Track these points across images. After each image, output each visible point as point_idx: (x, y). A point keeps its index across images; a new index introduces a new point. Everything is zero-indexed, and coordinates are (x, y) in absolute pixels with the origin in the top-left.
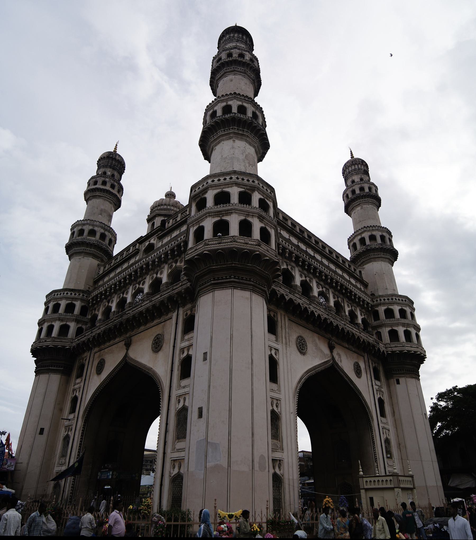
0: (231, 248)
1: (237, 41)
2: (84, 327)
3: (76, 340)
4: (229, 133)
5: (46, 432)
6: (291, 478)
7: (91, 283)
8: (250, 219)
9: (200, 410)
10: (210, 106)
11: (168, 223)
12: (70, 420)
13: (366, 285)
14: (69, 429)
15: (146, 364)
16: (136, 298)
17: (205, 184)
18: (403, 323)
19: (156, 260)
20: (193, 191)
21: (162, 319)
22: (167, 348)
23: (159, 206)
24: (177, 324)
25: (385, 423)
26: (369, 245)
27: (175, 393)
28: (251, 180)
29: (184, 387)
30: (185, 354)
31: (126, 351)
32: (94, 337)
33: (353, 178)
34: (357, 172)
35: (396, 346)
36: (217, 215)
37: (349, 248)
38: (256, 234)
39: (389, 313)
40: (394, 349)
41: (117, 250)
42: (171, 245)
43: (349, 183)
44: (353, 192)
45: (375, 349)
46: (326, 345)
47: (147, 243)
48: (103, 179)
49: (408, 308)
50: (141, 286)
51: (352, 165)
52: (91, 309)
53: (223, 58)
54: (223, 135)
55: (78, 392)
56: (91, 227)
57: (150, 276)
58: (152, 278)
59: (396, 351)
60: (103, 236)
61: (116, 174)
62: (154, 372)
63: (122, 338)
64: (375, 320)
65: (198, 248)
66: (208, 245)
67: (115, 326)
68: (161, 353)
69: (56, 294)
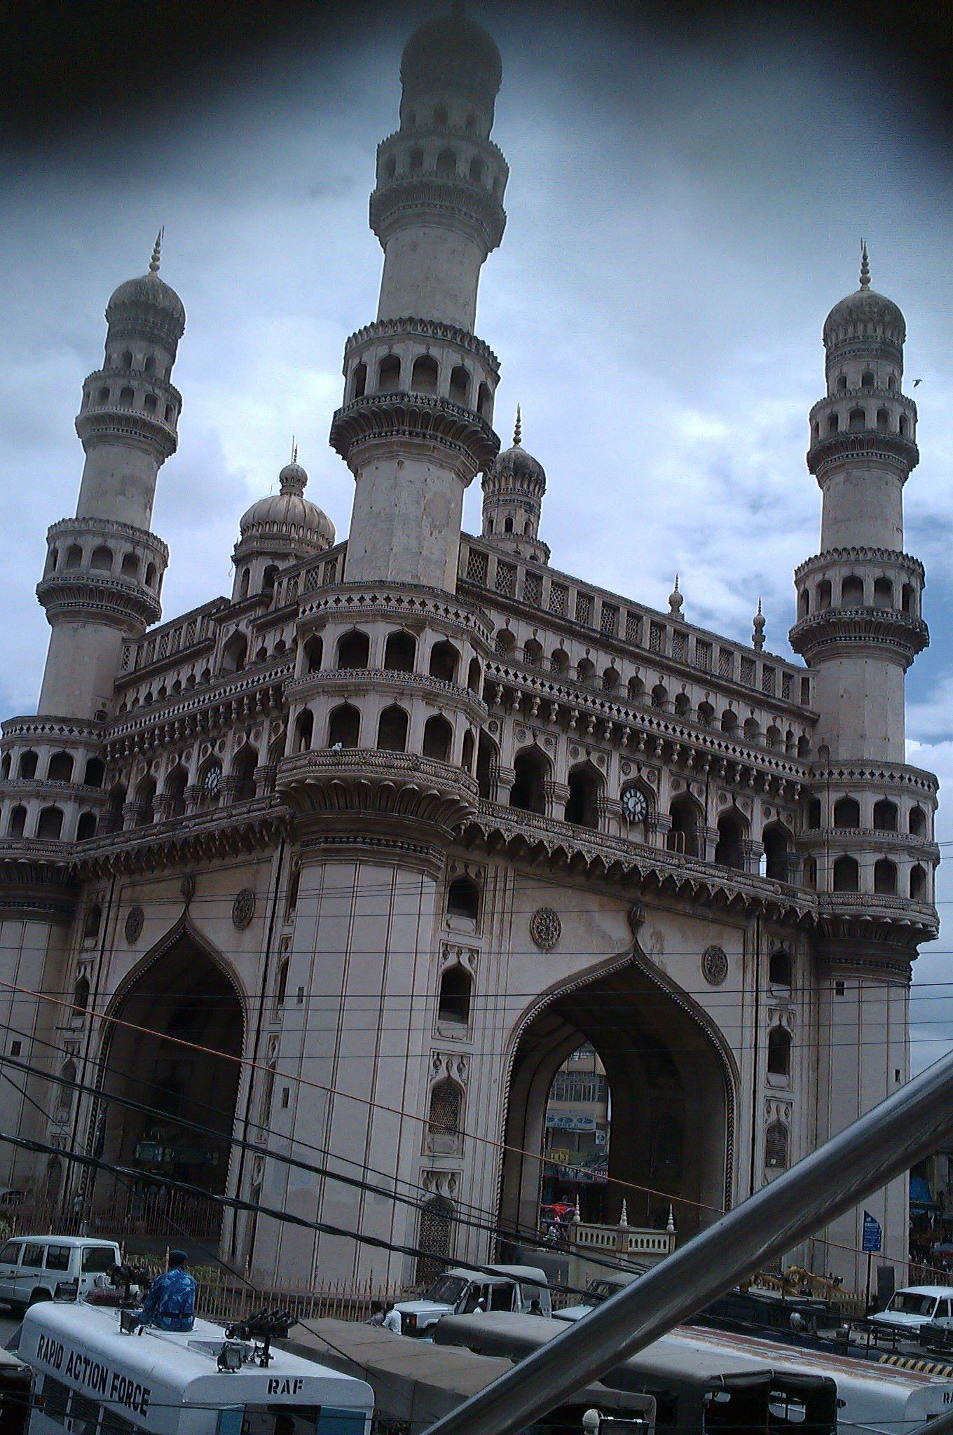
0: (355, 778)
2: (96, 812)
7: (109, 690)
8: (404, 704)
11: (280, 584)
13: (812, 722)
18: (876, 843)
19: (246, 701)
22: (259, 928)
24: (278, 879)
39: (847, 812)
40: (839, 910)
46: (622, 917)
48: (123, 382)
51: (847, 322)
55: (89, 970)
56: (97, 542)
58: (240, 739)
60: (131, 561)
61: (159, 354)
65: (298, 764)
66: (315, 765)
67: (161, 847)
68: (248, 933)
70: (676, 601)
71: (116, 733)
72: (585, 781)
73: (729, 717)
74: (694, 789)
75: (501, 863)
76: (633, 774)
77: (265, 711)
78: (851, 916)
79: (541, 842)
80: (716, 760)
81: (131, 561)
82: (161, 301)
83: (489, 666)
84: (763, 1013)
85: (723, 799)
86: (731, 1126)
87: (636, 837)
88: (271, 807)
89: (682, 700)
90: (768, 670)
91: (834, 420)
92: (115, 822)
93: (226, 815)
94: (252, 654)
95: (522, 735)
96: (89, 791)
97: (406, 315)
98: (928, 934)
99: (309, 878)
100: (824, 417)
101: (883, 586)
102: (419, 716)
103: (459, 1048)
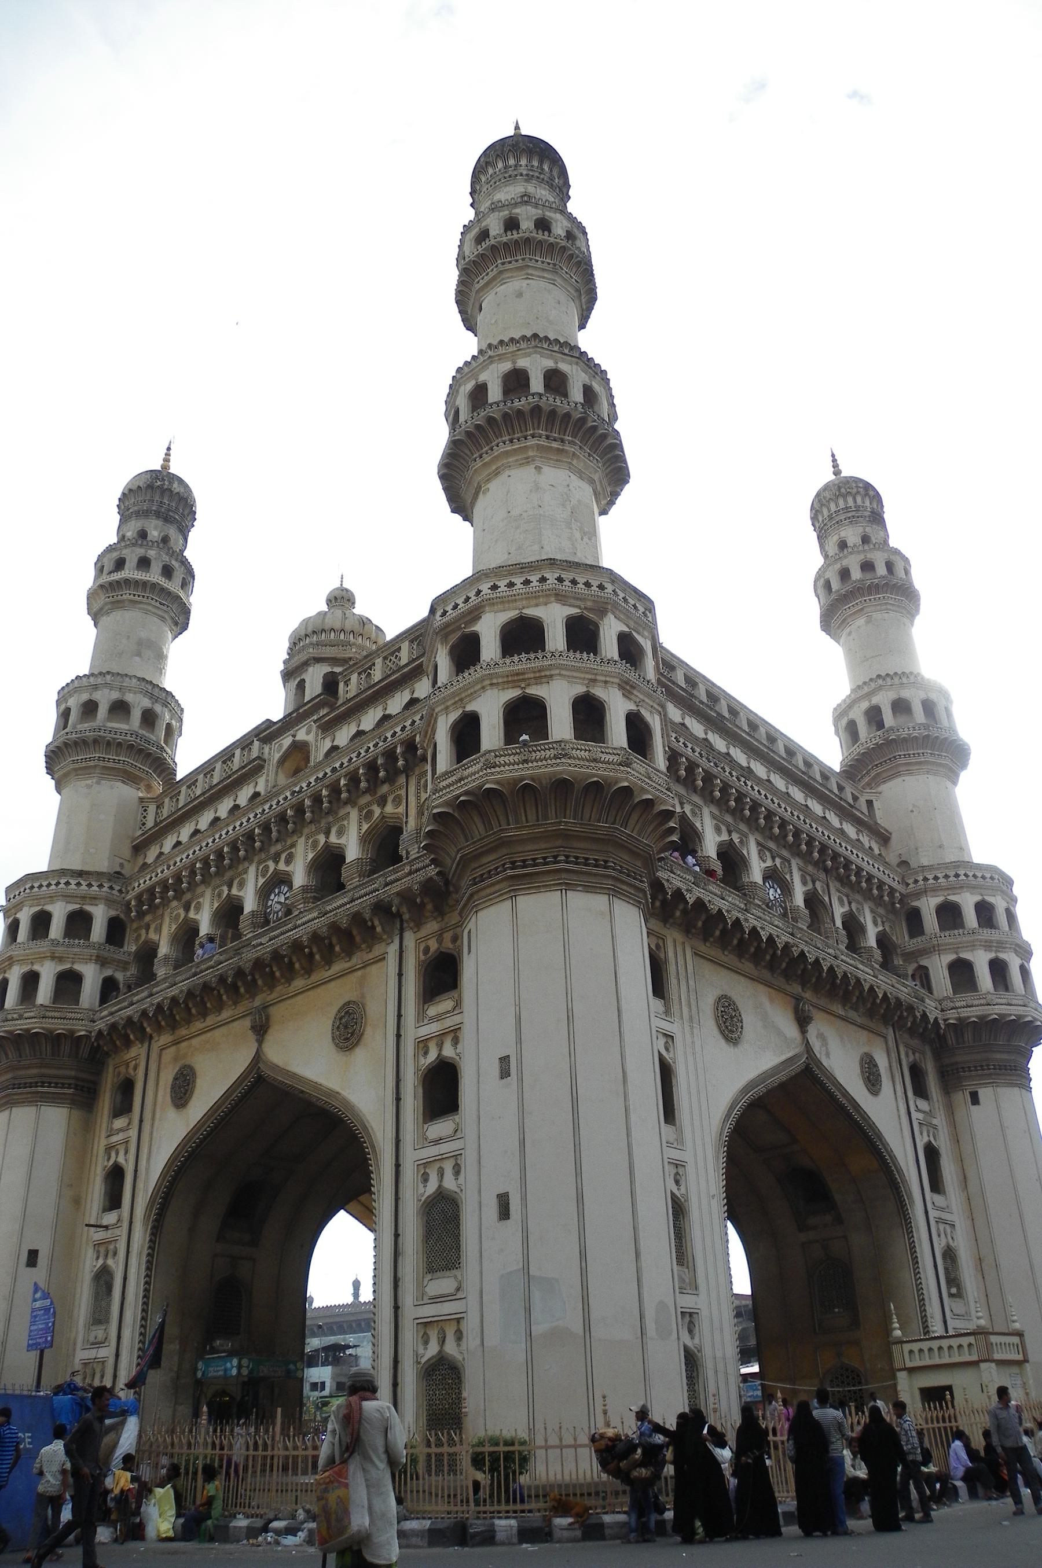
0: (555, 773)
2: (120, 976)
3: (105, 1013)
5: (42, 1259)
6: (719, 1354)
7: (127, 853)
8: (599, 692)
10: (466, 370)
11: (346, 684)
12: (106, 1227)
13: (884, 838)
14: (107, 1252)
15: (320, 1080)
16: (268, 899)
17: (472, 594)
20: (439, 613)
21: (356, 960)
22: (378, 1040)
23: (314, 632)
24: (400, 975)
26: (891, 729)
27: (410, 1157)
29: (438, 1141)
30: (432, 1056)
31: (256, 1045)
33: (843, 534)
34: (853, 516)
35: (970, 1003)
36: (514, 681)
37: (837, 733)
38: (618, 733)
39: (949, 914)
40: (965, 1013)
41: (189, 755)
42: (367, 751)
43: (832, 549)
44: (845, 574)
45: (915, 1017)
47: (287, 741)
48: (140, 552)
49: (999, 898)
50: (282, 866)
52: (135, 925)
53: (492, 233)
54: (507, 454)
55: (122, 1153)
56: (115, 695)
57: (308, 838)
58: (315, 843)
59: (969, 1017)
60: (149, 718)
62: (346, 1102)
63: (241, 1008)
64: (912, 936)
65: (466, 773)
67: (222, 979)
68: (360, 1053)
69: (36, 885)
75: (679, 937)
77: (351, 802)
78: (977, 1017)
79: (720, 910)
80: (836, 856)
86: (913, 1252)
88: (387, 885)
92: (146, 976)
93: (310, 921)
96: (111, 952)
102: (617, 709)
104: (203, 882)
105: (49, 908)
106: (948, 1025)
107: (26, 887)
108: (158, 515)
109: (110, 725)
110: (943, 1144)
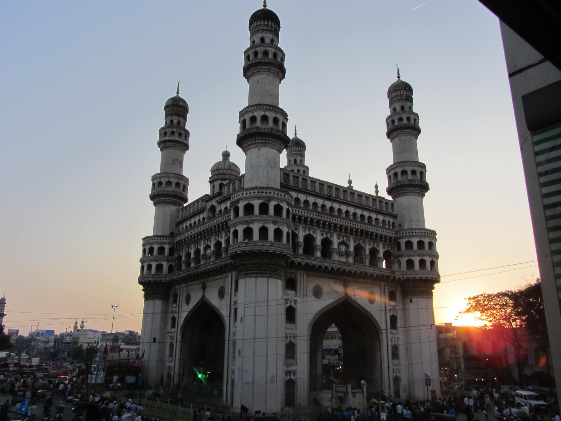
1: (263, 30)
2: (173, 264)
4: (256, 143)
5: (157, 340)
7: (174, 225)
8: (267, 225)
9: (240, 350)
13: (395, 217)
24: (231, 282)
25: (395, 334)
27: (232, 330)
28: (268, 192)
32: (181, 278)
38: (271, 236)
39: (409, 245)
40: (409, 276)
47: (211, 204)
48: (171, 130)
50: (209, 243)
56: (167, 180)
58: (216, 239)
60: (178, 184)
61: (181, 119)
68: (224, 300)
70: (350, 182)
71: (178, 239)
72: (326, 243)
73: (370, 218)
74: (361, 242)
75: (302, 272)
76: (341, 240)
77: (223, 230)
80: (367, 232)
81: (178, 184)
82: (181, 104)
83: (293, 210)
84: (388, 312)
85: (370, 244)
87: (343, 259)
89: (355, 214)
90: (381, 202)
91: (393, 121)
93: (212, 263)
94: (217, 212)
95: (305, 231)
97: (257, 103)
98: (437, 280)
99: (241, 282)
100: (390, 121)
101: (414, 172)
102: (271, 228)
103: (293, 332)
104: (192, 242)
105: (153, 246)
106: (404, 280)
107: (147, 240)
108: (176, 114)
109: (166, 189)
110: (399, 315)
